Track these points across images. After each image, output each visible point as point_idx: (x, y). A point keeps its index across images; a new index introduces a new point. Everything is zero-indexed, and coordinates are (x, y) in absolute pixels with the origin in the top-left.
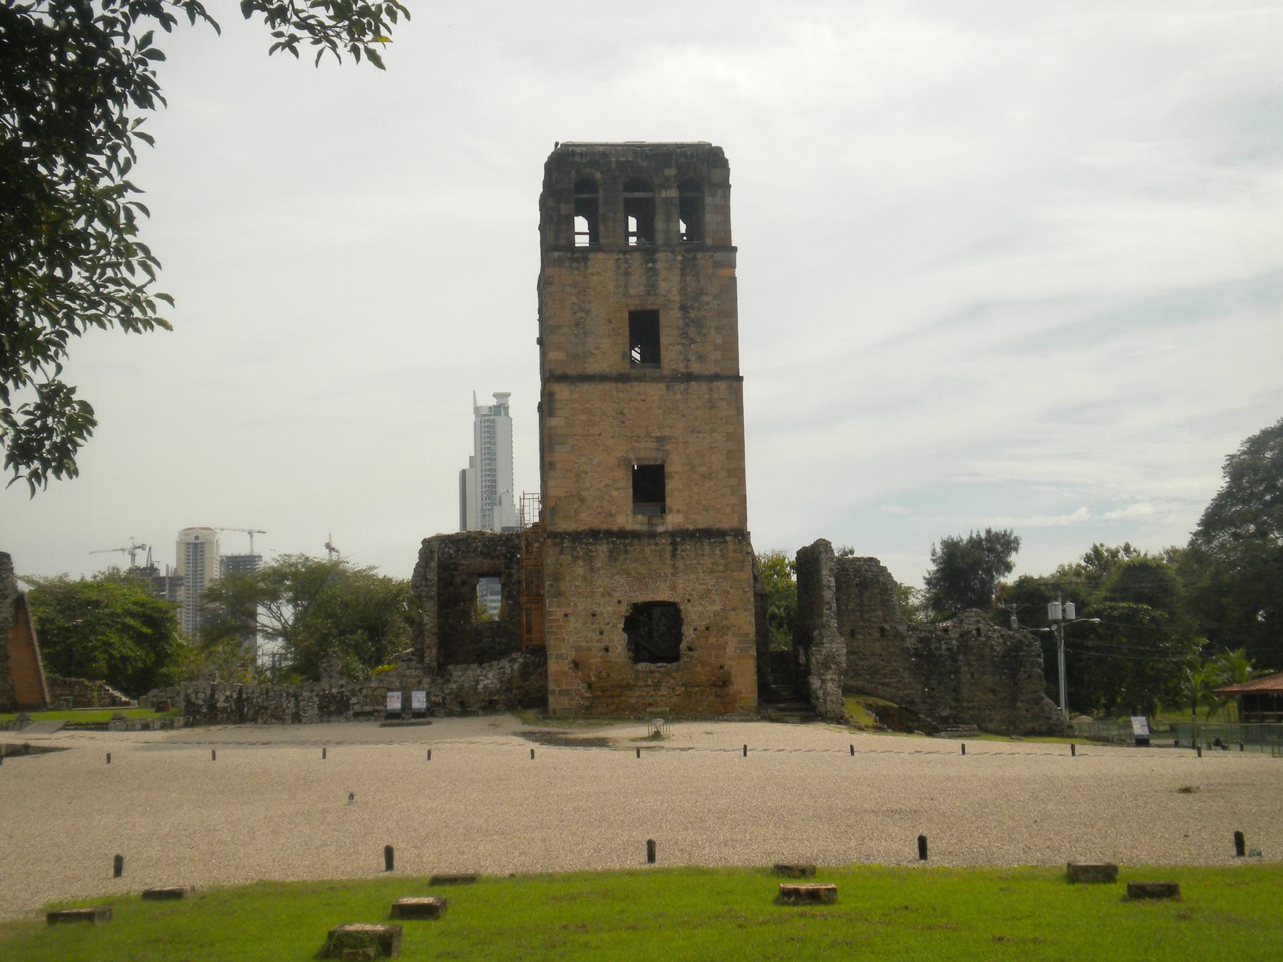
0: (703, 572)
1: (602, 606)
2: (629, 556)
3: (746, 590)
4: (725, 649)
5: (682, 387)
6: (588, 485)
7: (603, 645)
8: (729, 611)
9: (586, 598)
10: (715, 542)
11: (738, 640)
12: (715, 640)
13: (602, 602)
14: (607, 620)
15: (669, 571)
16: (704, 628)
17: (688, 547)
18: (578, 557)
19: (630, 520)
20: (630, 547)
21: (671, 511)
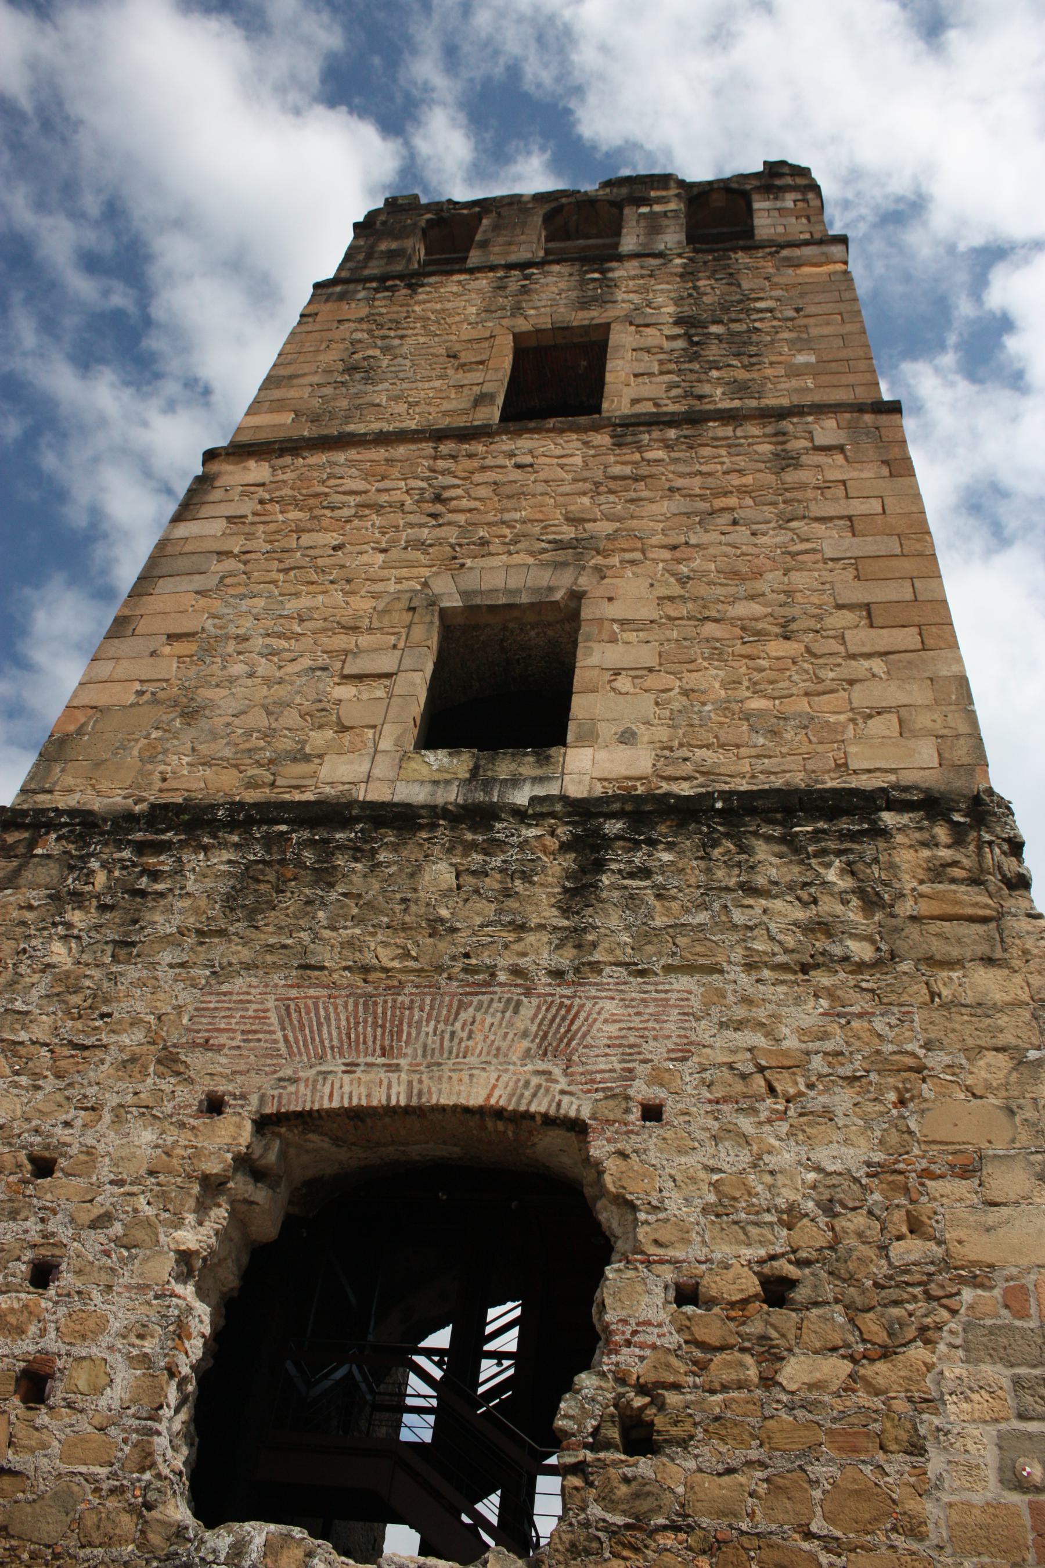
0: (750, 967)
1: (107, 1117)
2: (333, 896)
3: (1033, 1055)
4: (916, 1448)
5: (672, 433)
6: (238, 669)
7: (27, 1347)
8: (926, 1174)
9: (36, 1075)
10: (817, 835)
11: (1017, 1382)
12: (836, 1369)
13: (114, 1100)
14: (107, 1198)
15: (547, 958)
16: (752, 1285)
17: (666, 857)
18: (77, 899)
19: (383, 768)
20: (357, 860)
21: (589, 738)
